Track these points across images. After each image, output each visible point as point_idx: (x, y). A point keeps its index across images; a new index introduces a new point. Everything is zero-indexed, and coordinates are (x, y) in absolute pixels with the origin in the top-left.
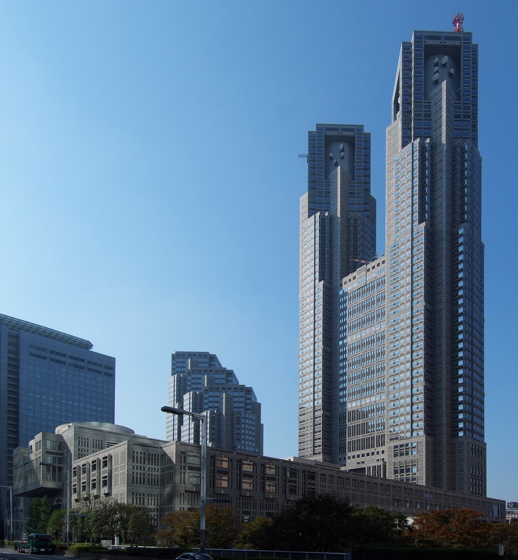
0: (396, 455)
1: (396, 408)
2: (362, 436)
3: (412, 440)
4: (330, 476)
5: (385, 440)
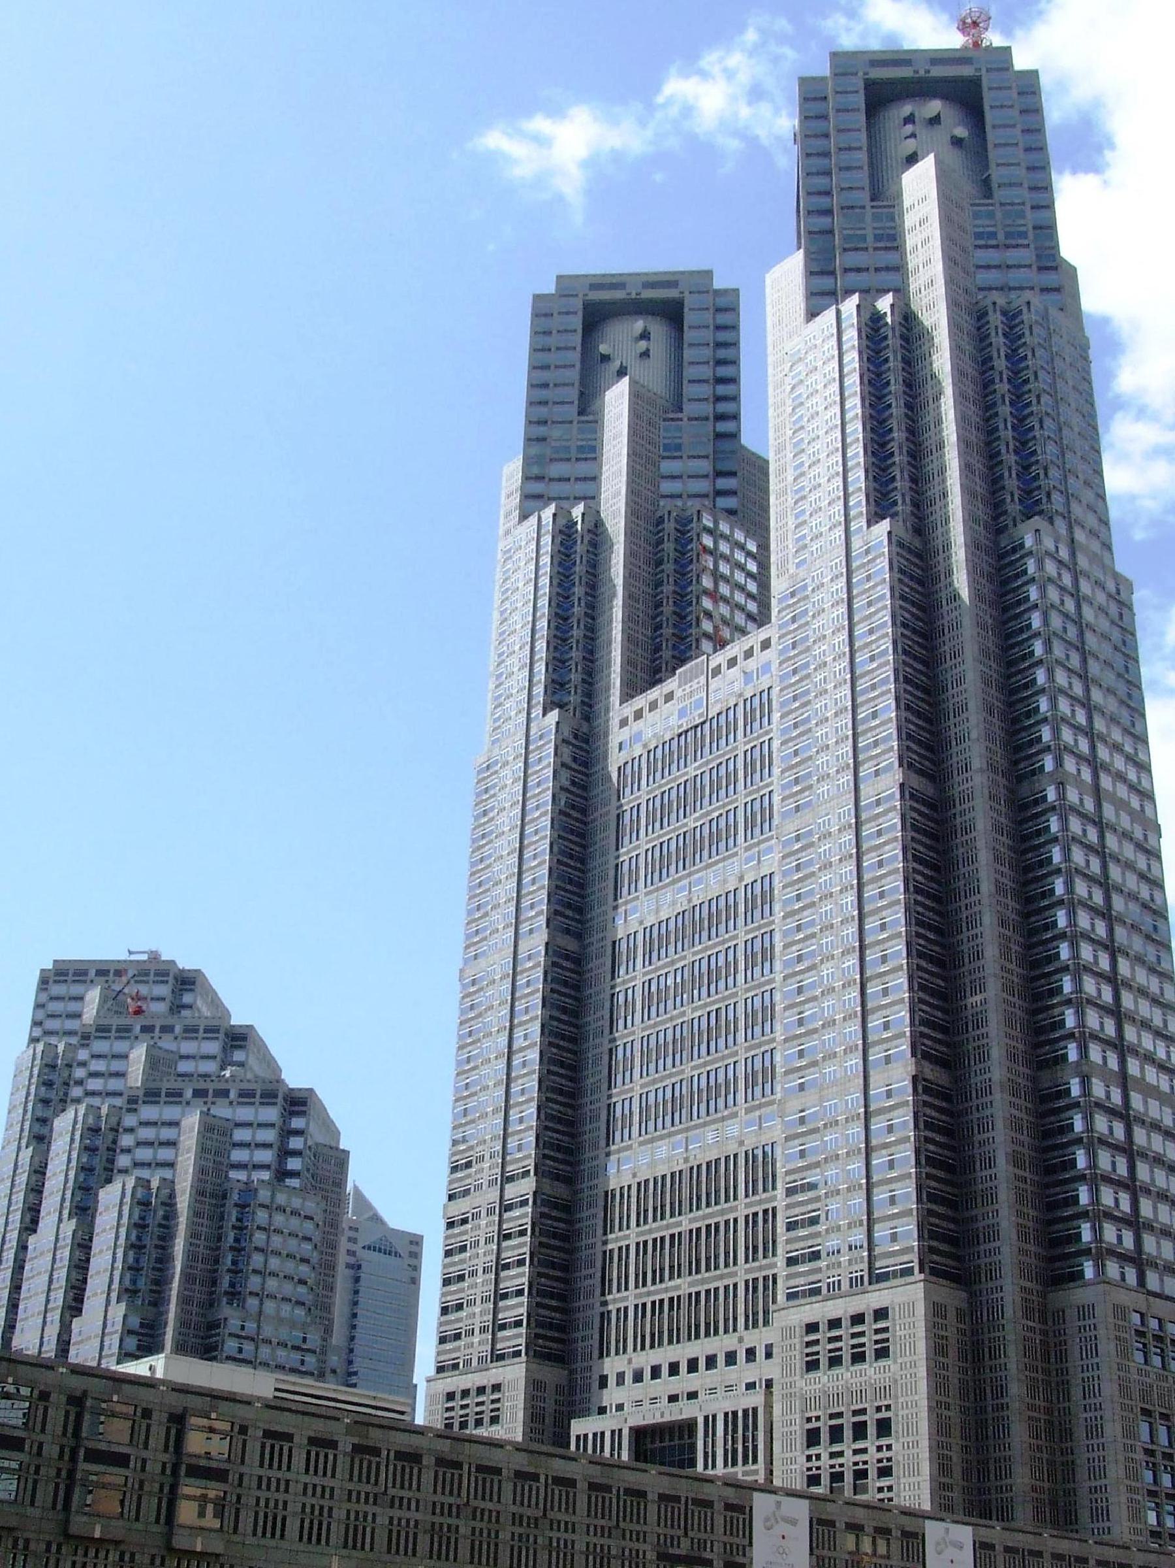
0: (812, 1366)
4: (313, 1441)
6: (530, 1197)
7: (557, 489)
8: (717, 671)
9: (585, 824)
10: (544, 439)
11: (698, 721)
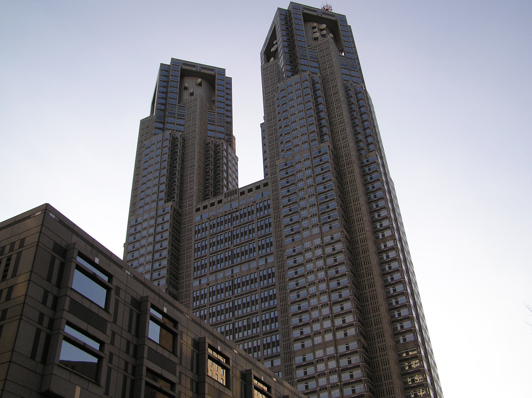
9: (179, 246)
11: (234, 210)
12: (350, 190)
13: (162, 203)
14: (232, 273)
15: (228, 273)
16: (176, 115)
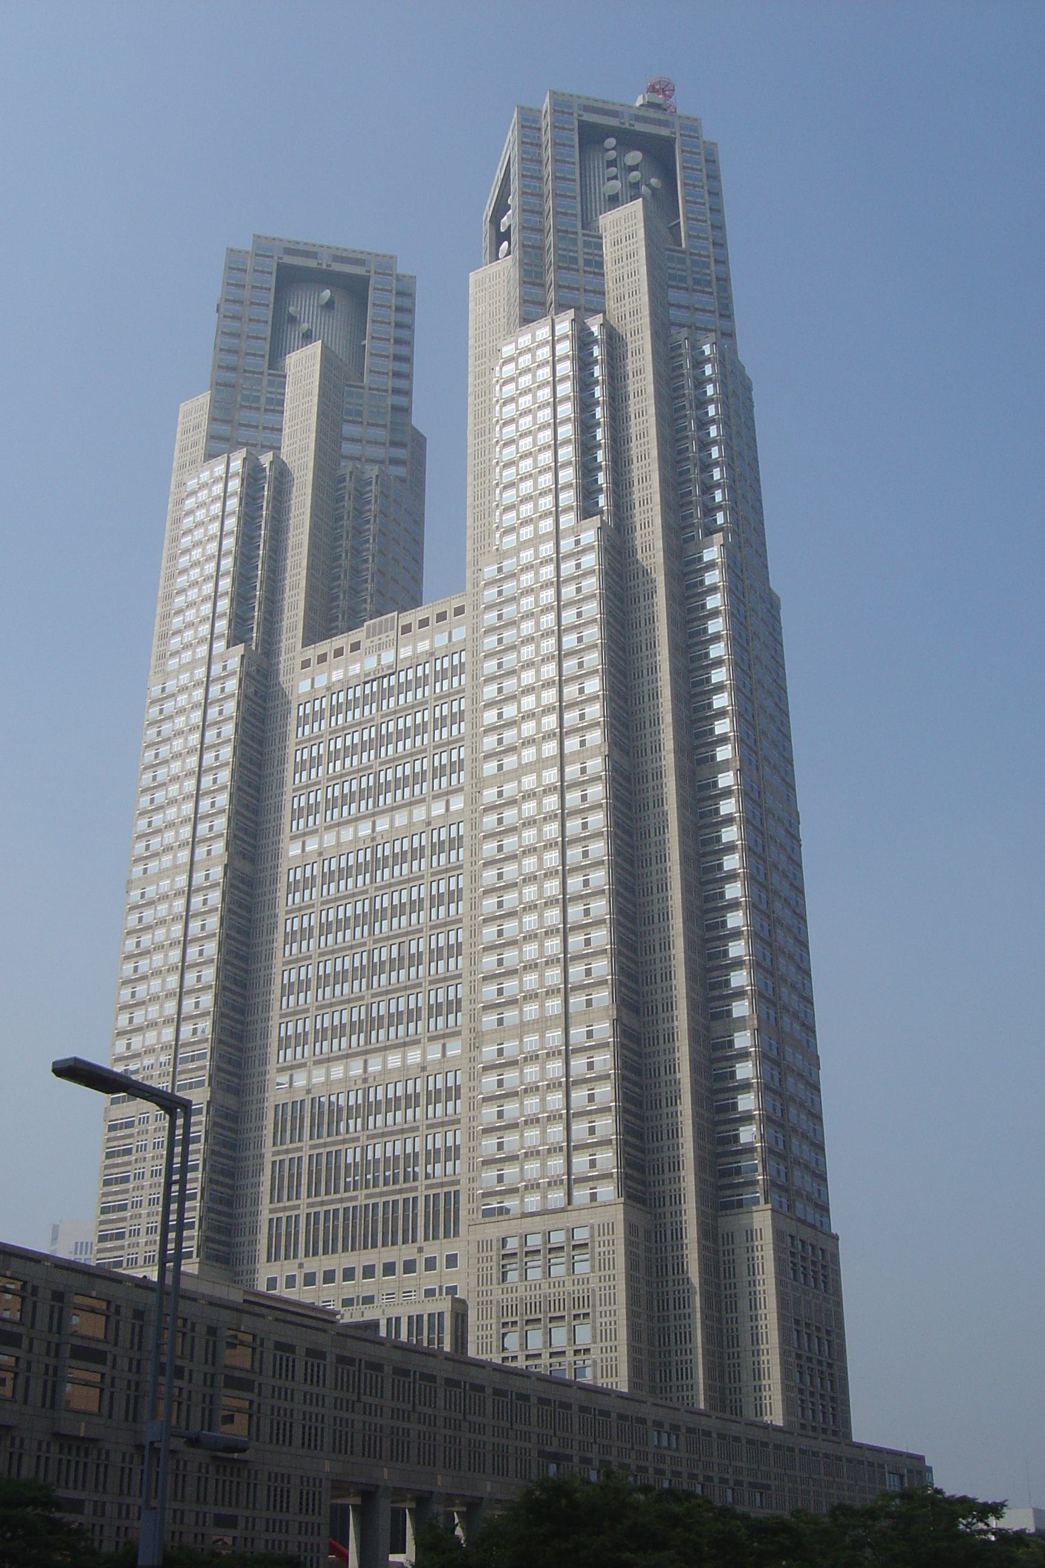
1: (506, 1096)
2: (368, 1197)
3: (570, 1219)
5: (462, 1213)
6: (204, 1106)
7: (244, 434)
8: (407, 629)
10: (233, 386)
12: (644, 642)
13: (220, 646)
14: (374, 830)
15: (365, 829)
16: (263, 401)
